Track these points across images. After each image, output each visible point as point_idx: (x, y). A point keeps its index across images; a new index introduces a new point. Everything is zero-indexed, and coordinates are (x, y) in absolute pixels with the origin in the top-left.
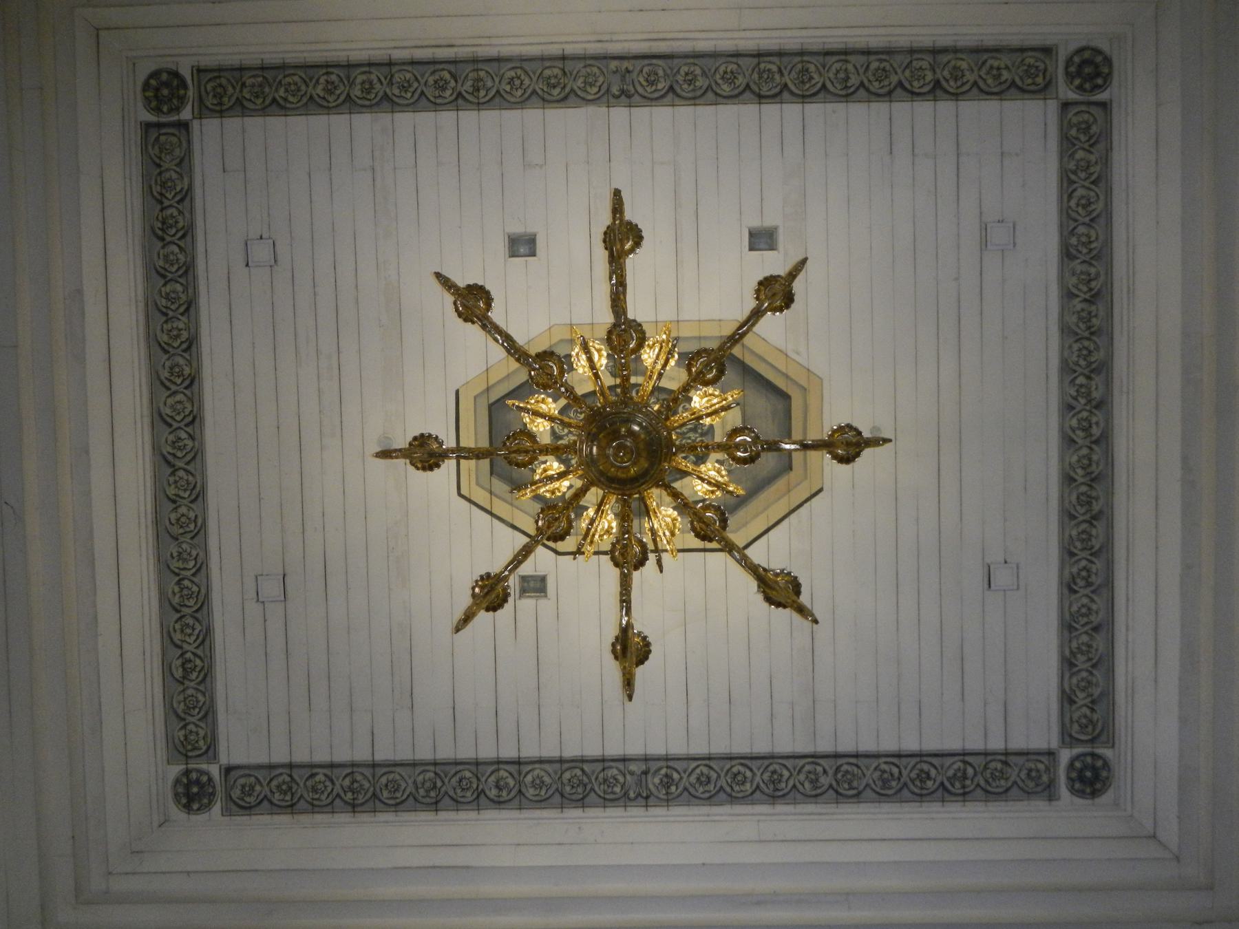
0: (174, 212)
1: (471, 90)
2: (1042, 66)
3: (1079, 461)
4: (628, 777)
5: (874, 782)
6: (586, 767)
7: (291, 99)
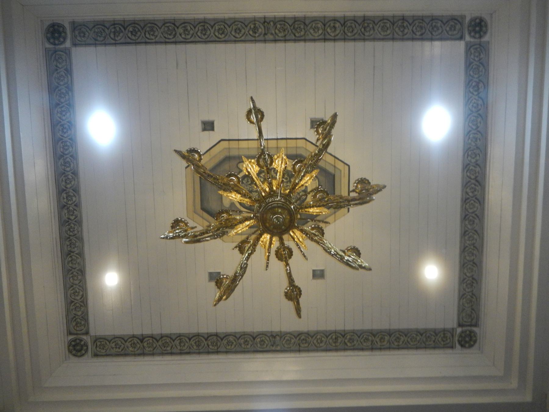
0: (467, 290)
1: (339, 338)
2: (98, 349)
3: (71, 182)
4: (273, 32)
5: (157, 30)
6: (294, 37)
7: (415, 336)
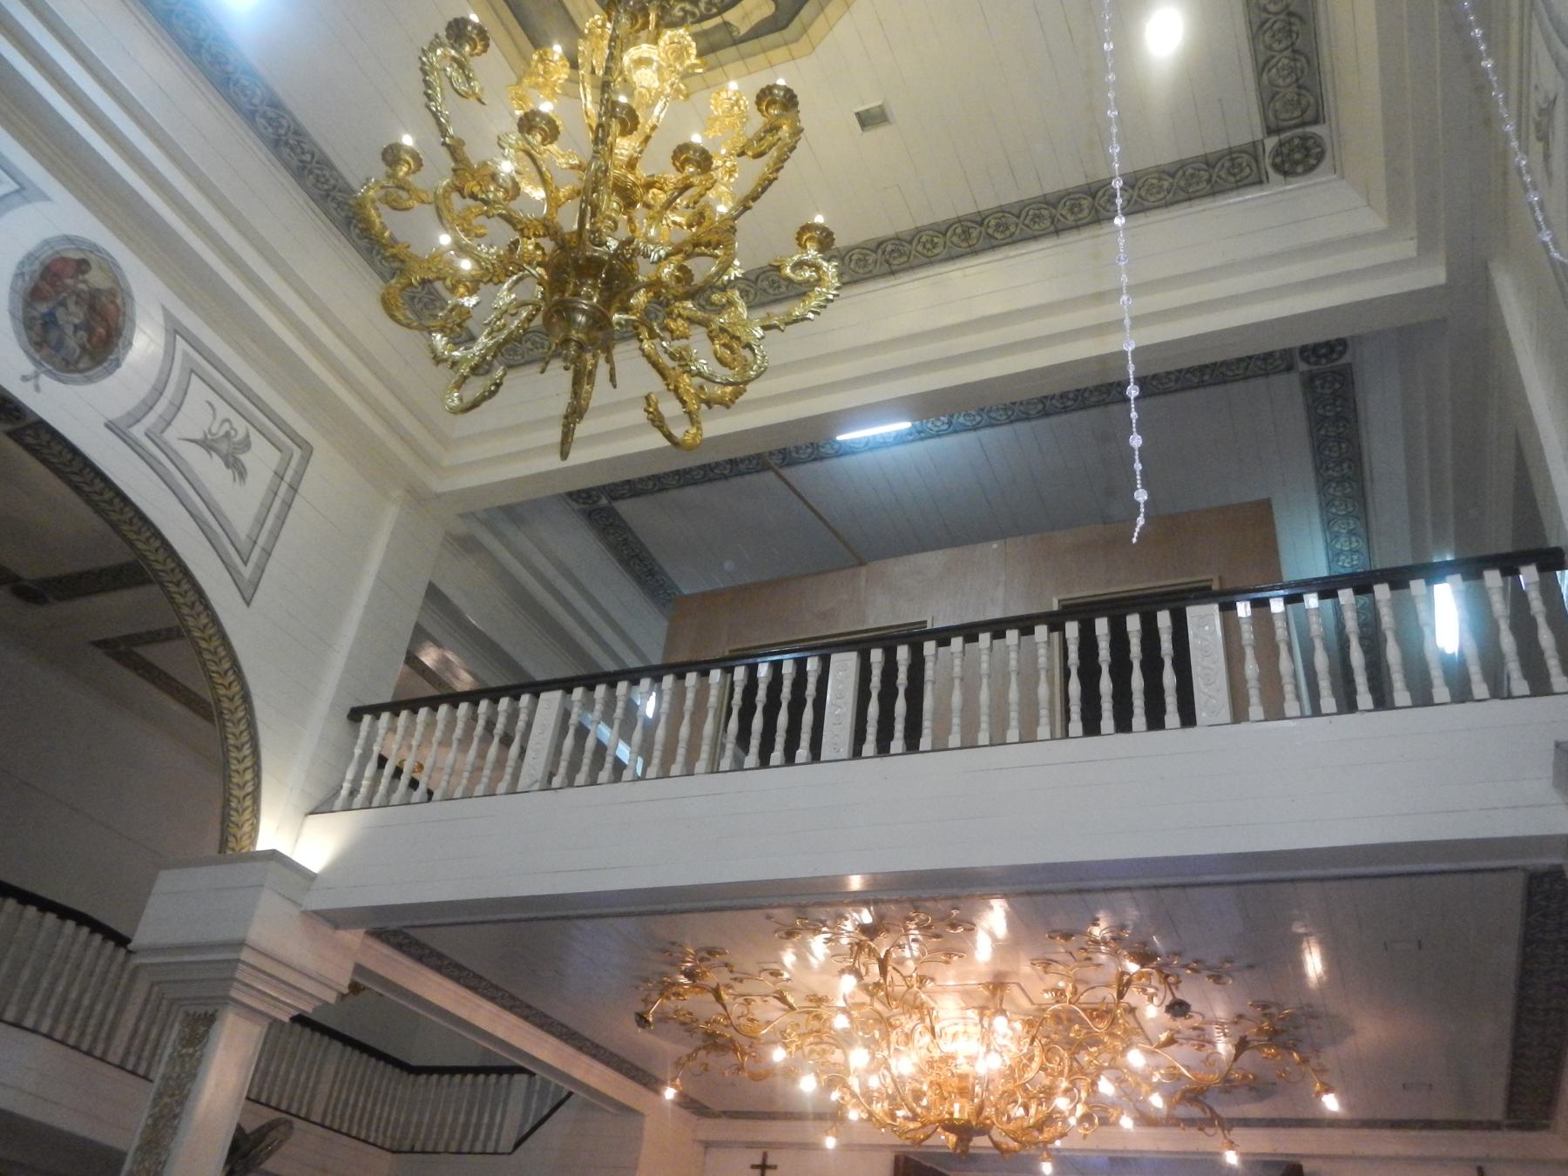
0: (1276, 46)
7: (1155, 181)
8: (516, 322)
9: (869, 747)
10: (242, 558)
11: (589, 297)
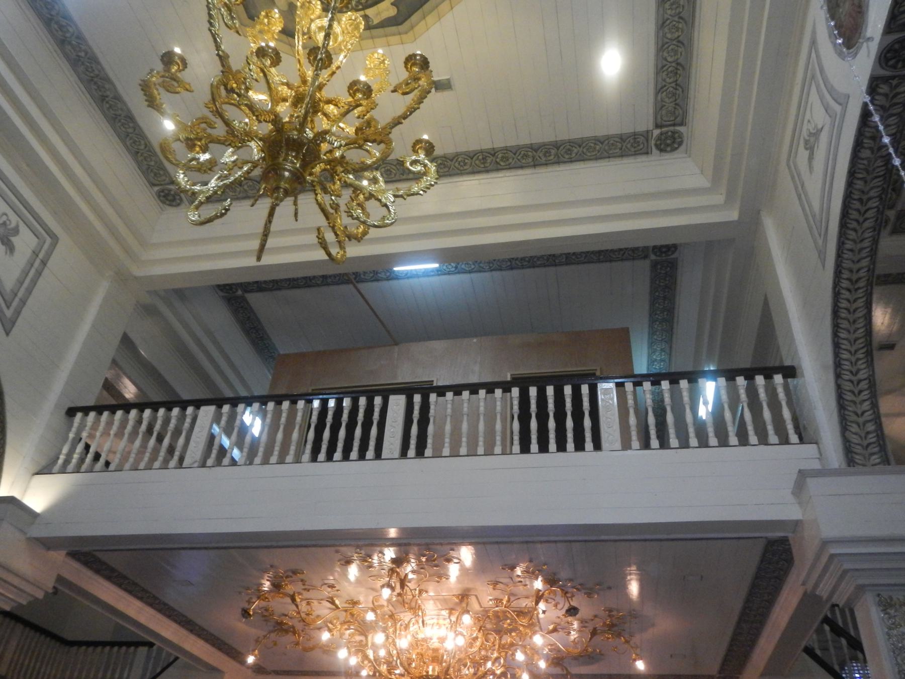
1: (487, 158)
7: (592, 145)
8: (240, 173)
9: (412, 452)
10: (6, 304)
11: (291, 164)
